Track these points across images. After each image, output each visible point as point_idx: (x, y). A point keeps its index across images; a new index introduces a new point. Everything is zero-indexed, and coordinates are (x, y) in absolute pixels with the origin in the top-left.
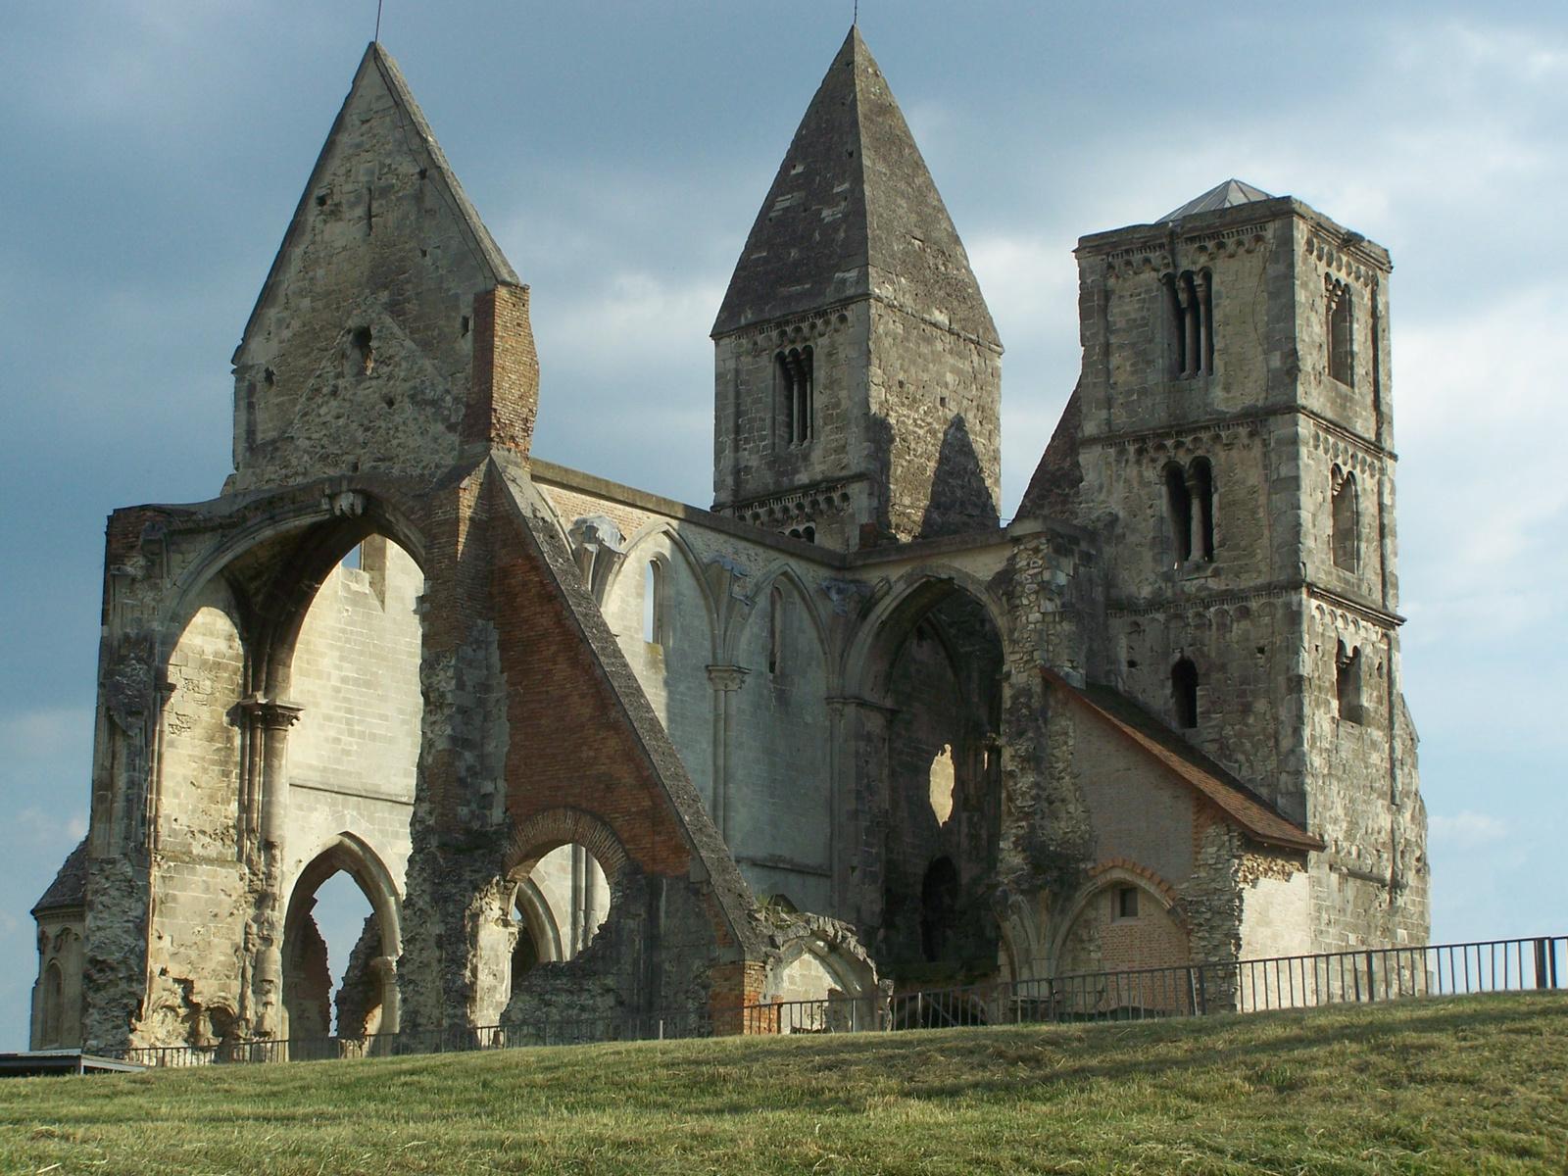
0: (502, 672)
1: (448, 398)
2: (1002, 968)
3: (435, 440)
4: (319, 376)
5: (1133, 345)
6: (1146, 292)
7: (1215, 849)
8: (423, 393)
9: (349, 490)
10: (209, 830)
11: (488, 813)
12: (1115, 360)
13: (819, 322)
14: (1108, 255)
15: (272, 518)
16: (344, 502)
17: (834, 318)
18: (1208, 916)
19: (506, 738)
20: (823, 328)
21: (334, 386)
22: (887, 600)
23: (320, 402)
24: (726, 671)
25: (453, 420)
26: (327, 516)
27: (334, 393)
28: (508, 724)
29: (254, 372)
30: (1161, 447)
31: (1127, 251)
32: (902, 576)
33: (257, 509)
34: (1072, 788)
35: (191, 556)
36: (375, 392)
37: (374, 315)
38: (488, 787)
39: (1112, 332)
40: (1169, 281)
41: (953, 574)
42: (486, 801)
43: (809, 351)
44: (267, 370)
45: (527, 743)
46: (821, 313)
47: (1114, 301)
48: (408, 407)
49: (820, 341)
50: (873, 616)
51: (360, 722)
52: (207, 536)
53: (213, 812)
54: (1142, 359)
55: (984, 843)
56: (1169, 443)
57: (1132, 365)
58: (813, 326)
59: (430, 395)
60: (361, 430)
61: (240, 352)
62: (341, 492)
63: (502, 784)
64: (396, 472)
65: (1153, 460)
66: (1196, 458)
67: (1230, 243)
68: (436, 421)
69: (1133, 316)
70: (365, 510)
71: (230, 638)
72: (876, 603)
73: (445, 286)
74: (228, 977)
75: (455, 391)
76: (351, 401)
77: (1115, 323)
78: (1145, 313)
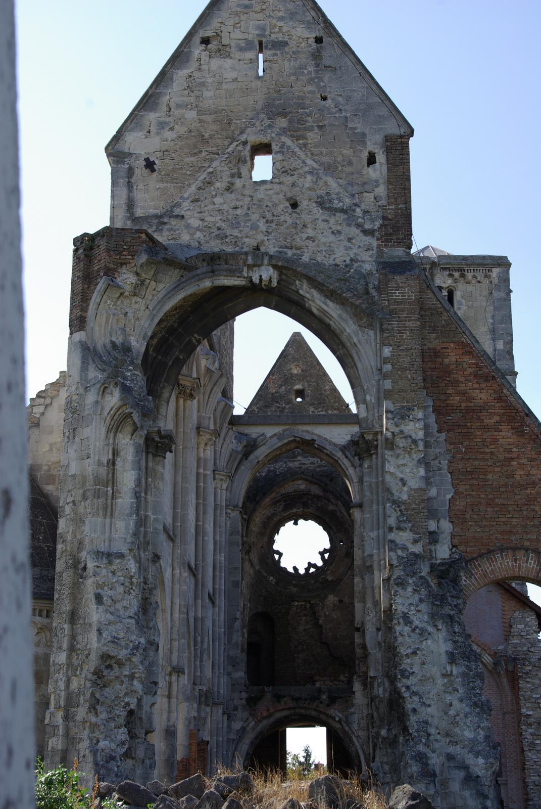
0: (439, 431)
1: (358, 210)
2: (356, 693)
3: (350, 240)
4: (210, 173)
7: (523, 626)
8: (330, 201)
9: (269, 265)
11: (433, 548)
15: (213, 272)
18: (530, 668)
19: (450, 487)
21: (229, 182)
23: (214, 193)
24: (224, 475)
26: (244, 283)
27: (229, 189)
28: (449, 475)
29: (133, 159)
32: (275, 435)
33: (204, 260)
35: (161, 286)
36: (278, 193)
37: (273, 135)
38: (432, 526)
41: (315, 437)
42: (434, 537)
44: (147, 160)
45: (474, 493)
48: (318, 213)
50: (252, 457)
62: (262, 265)
63: (446, 526)
64: (305, 258)
67: (469, 276)
68: (349, 225)
73: (350, 125)
75: (363, 207)
76: (252, 197)
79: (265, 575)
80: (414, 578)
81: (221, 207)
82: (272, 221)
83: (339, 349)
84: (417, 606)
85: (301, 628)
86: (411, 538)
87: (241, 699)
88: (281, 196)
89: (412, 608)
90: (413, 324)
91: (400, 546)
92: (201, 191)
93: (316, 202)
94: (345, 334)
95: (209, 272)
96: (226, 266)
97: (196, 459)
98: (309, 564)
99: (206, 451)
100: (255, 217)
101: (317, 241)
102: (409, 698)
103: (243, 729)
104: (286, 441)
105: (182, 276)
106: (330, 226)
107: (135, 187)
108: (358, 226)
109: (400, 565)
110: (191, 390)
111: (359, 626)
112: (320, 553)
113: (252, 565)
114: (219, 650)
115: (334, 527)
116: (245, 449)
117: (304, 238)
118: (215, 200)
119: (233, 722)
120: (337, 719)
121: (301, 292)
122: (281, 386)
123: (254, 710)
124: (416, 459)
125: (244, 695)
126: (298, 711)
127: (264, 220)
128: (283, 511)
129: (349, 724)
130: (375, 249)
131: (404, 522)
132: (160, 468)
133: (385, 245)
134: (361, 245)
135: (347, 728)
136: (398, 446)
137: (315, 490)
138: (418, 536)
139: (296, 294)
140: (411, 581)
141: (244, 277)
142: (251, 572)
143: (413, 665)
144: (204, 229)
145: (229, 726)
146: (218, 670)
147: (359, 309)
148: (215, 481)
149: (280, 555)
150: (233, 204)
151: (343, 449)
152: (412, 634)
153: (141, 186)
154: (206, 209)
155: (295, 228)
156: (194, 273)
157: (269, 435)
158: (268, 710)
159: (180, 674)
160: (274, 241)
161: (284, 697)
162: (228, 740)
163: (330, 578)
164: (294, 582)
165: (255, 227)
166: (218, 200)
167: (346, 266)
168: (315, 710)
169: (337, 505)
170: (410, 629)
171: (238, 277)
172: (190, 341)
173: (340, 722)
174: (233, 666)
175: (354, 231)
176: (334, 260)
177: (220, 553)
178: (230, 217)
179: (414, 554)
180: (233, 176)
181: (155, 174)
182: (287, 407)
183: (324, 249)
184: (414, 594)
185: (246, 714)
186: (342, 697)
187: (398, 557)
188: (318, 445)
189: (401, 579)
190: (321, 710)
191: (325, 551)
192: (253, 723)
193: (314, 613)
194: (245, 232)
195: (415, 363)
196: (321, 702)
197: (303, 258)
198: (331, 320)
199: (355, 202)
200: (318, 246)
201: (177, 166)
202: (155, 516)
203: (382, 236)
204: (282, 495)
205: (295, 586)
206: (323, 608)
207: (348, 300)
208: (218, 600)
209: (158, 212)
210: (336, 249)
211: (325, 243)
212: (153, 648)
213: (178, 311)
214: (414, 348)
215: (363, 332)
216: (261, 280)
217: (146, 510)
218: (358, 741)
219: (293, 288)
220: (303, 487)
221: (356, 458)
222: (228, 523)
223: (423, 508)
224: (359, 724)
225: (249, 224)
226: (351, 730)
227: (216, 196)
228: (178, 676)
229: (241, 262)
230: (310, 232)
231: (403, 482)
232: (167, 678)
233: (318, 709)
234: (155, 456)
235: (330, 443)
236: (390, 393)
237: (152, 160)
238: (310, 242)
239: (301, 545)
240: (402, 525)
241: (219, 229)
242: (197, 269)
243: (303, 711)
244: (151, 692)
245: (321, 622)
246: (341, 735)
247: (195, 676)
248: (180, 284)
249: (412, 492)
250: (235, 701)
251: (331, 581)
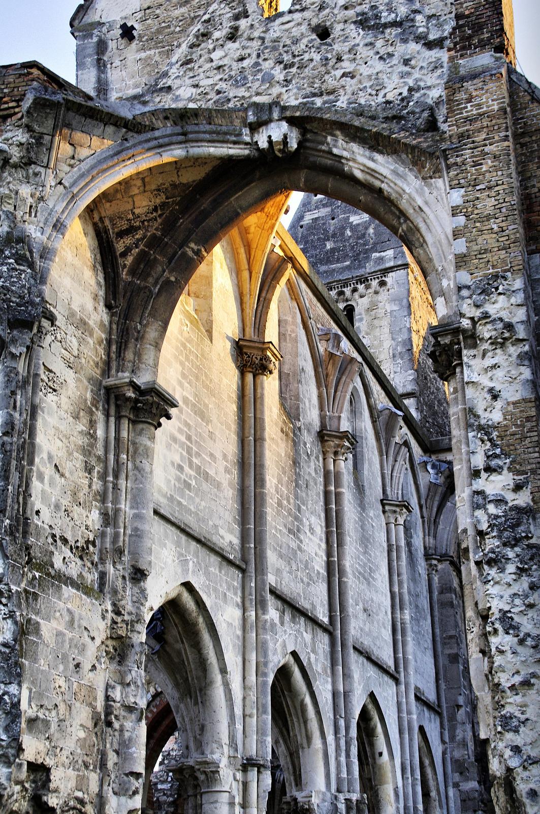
1: (419, 18)
3: (406, 62)
4: (205, 21)
8: (377, 17)
10: (69, 538)
13: (361, 287)
15: (184, 134)
16: (277, 131)
17: (375, 283)
20: (364, 291)
21: (231, 27)
23: (211, 47)
25: (431, 37)
26: (247, 152)
27: (233, 36)
29: (104, 29)
33: (166, 118)
36: (299, 24)
43: (350, 310)
46: (363, 280)
48: (357, 36)
49: (360, 301)
51: (198, 455)
52: (110, 129)
53: (76, 517)
58: (355, 290)
59: (386, 17)
60: (279, 68)
61: (82, 10)
62: (270, 121)
64: (342, 103)
68: (405, 41)
70: (299, 144)
71: (95, 298)
74: (86, 766)
75: (428, 11)
80: (517, 549)
81: (221, 63)
82: (292, 65)
83: (400, 224)
84: (527, 597)
86: (512, 483)
88: (304, 28)
89: (517, 601)
90: (498, 146)
91: (492, 498)
92: (195, 49)
93: (355, 22)
94: (405, 196)
95: (178, 134)
96: (208, 127)
97: (322, 474)
99: (338, 462)
100: (266, 66)
101: (358, 77)
102: (520, 770)
105: (126, 140)
106: (375, 49)
107: (109, 66)
108: (418, 39)
109: (492, 530)
110: (261, 359)
114: (411, 747)
117: (338, 77)
118: (213, 56)
121: (335, 151)
124: (515, 355)
127: (282, 66)
130: (445, 65)
131: (496, 456)
132: (144, 441)
133: (462, 56)
134: (424, 65)
136: (482, 339)
138: (521, 477)
139: (329, 156)
140: (511, 554)
141: (247, 144)
143: (526, 706)
144: (199, 97)
146: (412, 775)
147: (416, 151)
148: (386, 515)
150: (237, 55)
152: (520, 649)
153: (117, 63)
154: (201, 70)
155: (325, 65)
156: (149, 135)
159: (262, 769)
160: (295, 91)
165: (269, 79)
166: (216, 55)
167: (402, 100)
170: (516, 639)
171: (235, 143)
172: (184, 254)
174: (461, 773)
175: (413, 47)
176: (385, 96)
177: (401, 609)
178: (233, 73)
179: (516, 508)
180: (237, 17)
181: (135, 42)
183: (368, 85)
184: (520, 576)
187: (489, 516)
189: (494, 552)
194: (254, 88)
195: (504, 205)
197: (338, 104)
198: (383, 182)
199: (414, 7)
200: (360, 82)
201: (163, 25)
202: (136, 511)
203: (455, 44)
207: (399, 141)
208: (402, 674)
209: (139, 91)
210: (386, 80)
211: (370, 76)
212: (133, 717)
213: (159, 212)
214: (500, 182)
215: (429, 186)
216: (270, 141)
217: (116, 501)
219: (323, 148)
222: (436, 579)
223: (530, 431)
225: (259, 76)
227: (214, 49)
228: (259, 772)
229: (237, 122)
230: (347, 66)
231: (495, 396)
232: (239, 775)
234: (134, 422)
236: (465, 259)
237: (129, 25)
238: (349, 79)
240: (493, 463)
241: (218, 92)
242: (153, 129)
244: (127, 790)
247: (339, 780)
248: (122, 151)
249: (511, 408)
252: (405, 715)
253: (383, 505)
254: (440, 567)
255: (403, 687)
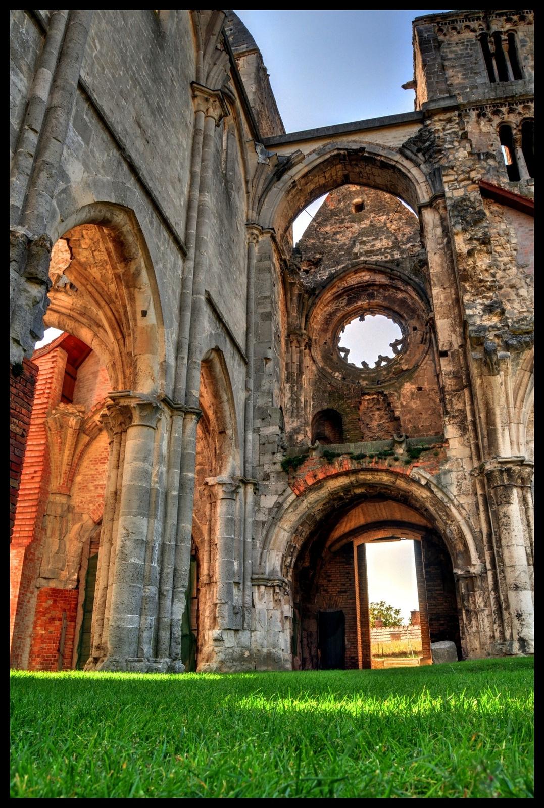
2: (451, 442)
5: (463, 66)
6: (467, 42)
12: (450, 72)
14: (438, 23)
22: (299, 166)
30: (496, 112)
31: (453, 22)
32: (314, 151)
34: (520, 276)
39: (445, 60)
40: (483, 39)
41: (363, 145)
47: (444, 45)
50: (286, 177)
54: (470, 71)
55: (302, 405)
56: (504, 109)
57: (463, 75)
65: (490, 120)
66: (525, 119)
69: (459, 52)
72: (290, 168)
77: (447, 56)
78: (469, 51)
79: (330, 371)
85: (374, 424)
87: (275, 463)
98: (380, 357)
103: (279, 505)
104: (328, 156)
111: (445, 349)
112: (391, 345)
113: (314, 361)
115: (405, 315)
116: (276, 168)
119: (262, 497)
120: (423, 482)
122: (340, 201)
123: (294, 478)
125: (279, 457)
126: (362, 476)
128: (346, 305)
129: (442, 488)
135: (440, 495)
137: (381, 279)
142: (314, 368)
145: (257, 503)
149: (347, 351)
151: (401, 151)
157: (306, 152)
158: (315, 476)
161: (339, 455)
162: (256, 523)
163: (405, 367)
164: (363, 375)
168: (387, 471)
169: (406, 292)
173: (427, 486)
174: (263, 419)
177: (201, 191)
182: (347, 217)
185: (281, 485)
186: (428, 449)
188: (369, 153)
190: (398, 470)
191: (398, 342)
192: (293, 497)
193: (389, 404)
196: (396, 459)
204: (344, 288)
205: (364, 379)
206: (399, 399)
218: (460, 513)
220: (367, 278)
221: (420, 154)
224: (459, 486)
226: (447, 496)
233: (392, 469)
235: (384, 148)
239: (368, 340)
243: (369, 477)
245: (397, 413)
246: (432, 508)
250: (266, 467)
251: (407, 370)
252: (189, 292)
253: (193, 90)
254: (260, 239)
255: (191, 264)
